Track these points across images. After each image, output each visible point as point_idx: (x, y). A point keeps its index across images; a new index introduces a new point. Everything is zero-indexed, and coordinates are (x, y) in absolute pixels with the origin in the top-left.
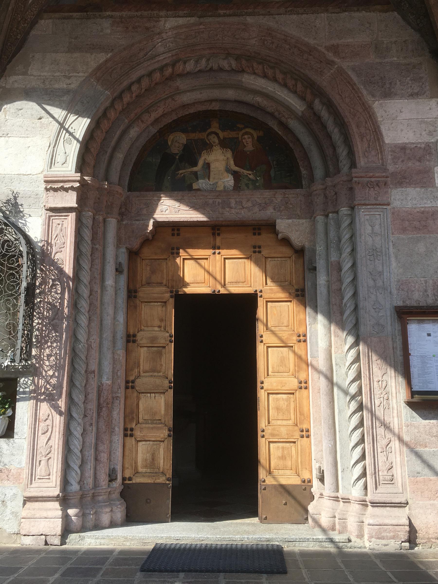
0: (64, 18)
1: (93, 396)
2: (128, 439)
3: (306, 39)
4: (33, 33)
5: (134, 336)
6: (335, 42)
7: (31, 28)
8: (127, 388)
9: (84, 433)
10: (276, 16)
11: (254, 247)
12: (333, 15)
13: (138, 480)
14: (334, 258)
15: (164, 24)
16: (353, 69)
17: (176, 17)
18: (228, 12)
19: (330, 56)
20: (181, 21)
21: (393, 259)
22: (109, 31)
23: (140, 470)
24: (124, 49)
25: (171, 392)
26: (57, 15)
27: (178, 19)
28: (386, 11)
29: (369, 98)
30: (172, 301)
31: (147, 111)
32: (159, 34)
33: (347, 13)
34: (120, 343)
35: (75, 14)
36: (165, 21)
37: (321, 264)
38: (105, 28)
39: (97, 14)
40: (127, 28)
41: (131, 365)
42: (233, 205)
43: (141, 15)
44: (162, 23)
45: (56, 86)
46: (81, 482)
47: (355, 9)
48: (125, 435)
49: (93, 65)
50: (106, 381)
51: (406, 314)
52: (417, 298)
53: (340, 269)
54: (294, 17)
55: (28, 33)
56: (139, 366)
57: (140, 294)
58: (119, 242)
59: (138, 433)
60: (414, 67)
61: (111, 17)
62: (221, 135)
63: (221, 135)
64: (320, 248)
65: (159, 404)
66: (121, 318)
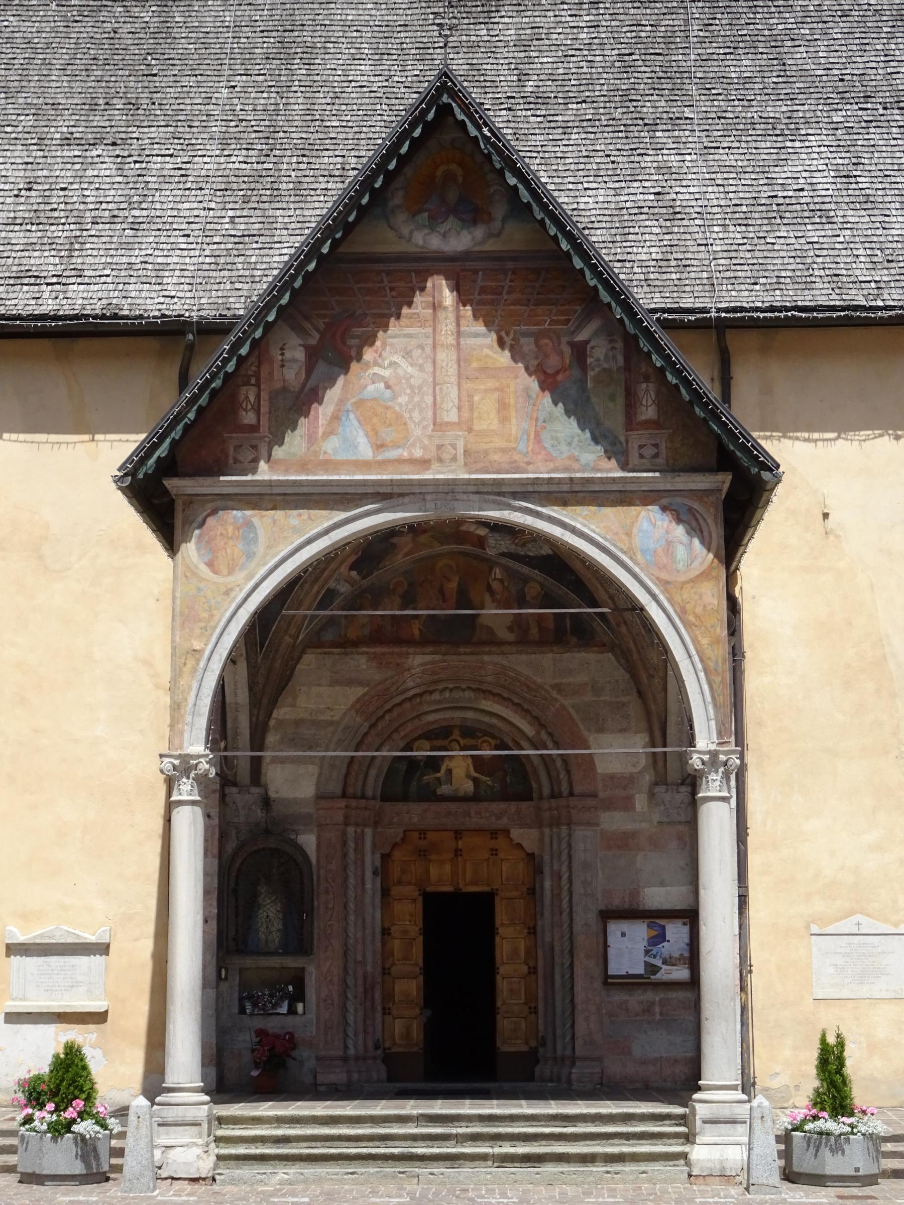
0: (325, 653)
1: (360, 982)
2: (387, 1017)
4: (298, 666)
5: (389, 929)
6: (557, 681)
7: (297, 663)
8: (384, 974)
9: (356, 1010)
11: (492, 850)
13: (395, 1050)
14: (555, 867)
16: (573, 707)
19: (555, 694)
20: (428, 658)
21: (600, 872)
22: (365, 667)
23: (398, 1041)
24: (379, 684)
25: (421, 978)
26: (319, 650)
29: (585, 733)
30: (421, 898)
31: (397, 730)
34: (378, 936)
37: (547, 870)
38: (360, 663)
41: (386, 954)
42: (473, 814)
44: (410, 660)
45: (322, 718)
46: (355, 1047)
48: (384, 1014)
49: (353, 699)
50: (369, 968)
51: (608, 915)
52: (616, 902)
53: (560, 878)
56: (393, 955)
57: (392, 892)
58: (374, 846)
59: (394, 1012)
60: (624, 705)
61: (367, 653)
62: (462, 742)
63: (462, 742)
64: (547, 858)
65: (410, 987)
66: (378, 915)
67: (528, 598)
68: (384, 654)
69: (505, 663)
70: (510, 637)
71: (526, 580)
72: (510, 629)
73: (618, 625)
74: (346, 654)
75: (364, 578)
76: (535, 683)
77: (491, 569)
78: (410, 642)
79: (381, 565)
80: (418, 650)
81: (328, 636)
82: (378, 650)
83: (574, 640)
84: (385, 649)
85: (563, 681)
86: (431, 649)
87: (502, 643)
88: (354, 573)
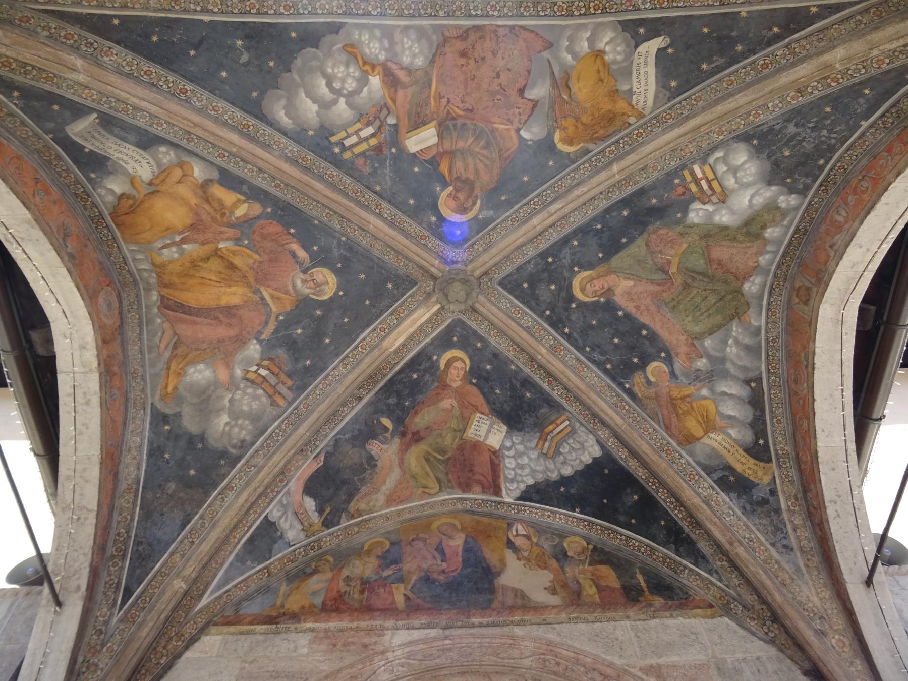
0: (241, 633)
3: (609, 658)
4: (188, 654)
7: (187, 648)
10: (556, 626)
12: (638, 623)
15: (391, 638)
17: (408, 629)
18: (485, 621)
20: (416, 634)
22: (305, 651)
26: (232, 629)
27: (413, 631)
28: (712, 617)
32: (383, 653)
33: (657, 621)
35: (259, 628)
36: (393, 635)
39: (292, 627)
40: (335, 645)
43: (357, 627)
44: (387, 638)
47: (667, 614)
54: (582, 626)
55: (178, 656)
61: (313, 630)
67: (569, 554)
68: (341, 631)
69: (551, 636)
70: (555, 600)
71: (563, 535)
72: (553, 591)
73: (731, 544)
74: (277, 633)
75: (327, 524)
76: (611, 665)
77: (510, 525)
78: (390, 611)
79: (352, 507)
80: (400, 623)
81: (253, 608)
82: (334, 624)
83: (659, 601)
84: (345, 623)
85: (661, 661)
86: (424, 620)
87: (539, 608)
88: (310, 503)
